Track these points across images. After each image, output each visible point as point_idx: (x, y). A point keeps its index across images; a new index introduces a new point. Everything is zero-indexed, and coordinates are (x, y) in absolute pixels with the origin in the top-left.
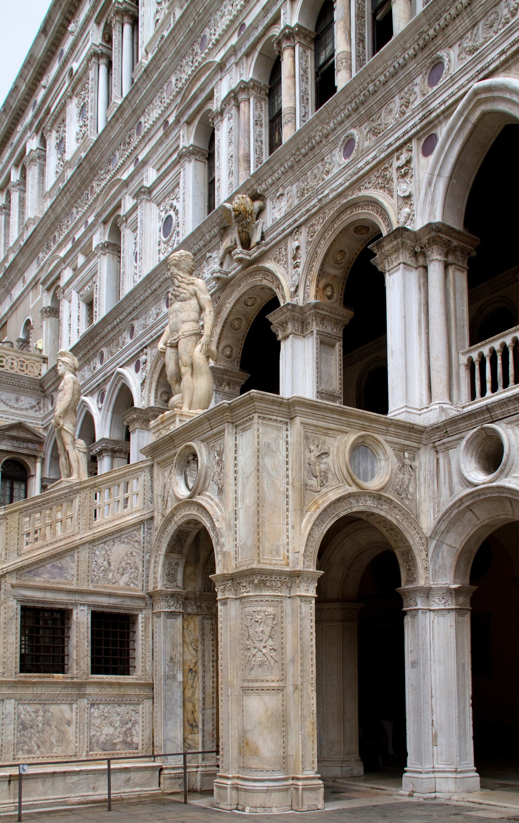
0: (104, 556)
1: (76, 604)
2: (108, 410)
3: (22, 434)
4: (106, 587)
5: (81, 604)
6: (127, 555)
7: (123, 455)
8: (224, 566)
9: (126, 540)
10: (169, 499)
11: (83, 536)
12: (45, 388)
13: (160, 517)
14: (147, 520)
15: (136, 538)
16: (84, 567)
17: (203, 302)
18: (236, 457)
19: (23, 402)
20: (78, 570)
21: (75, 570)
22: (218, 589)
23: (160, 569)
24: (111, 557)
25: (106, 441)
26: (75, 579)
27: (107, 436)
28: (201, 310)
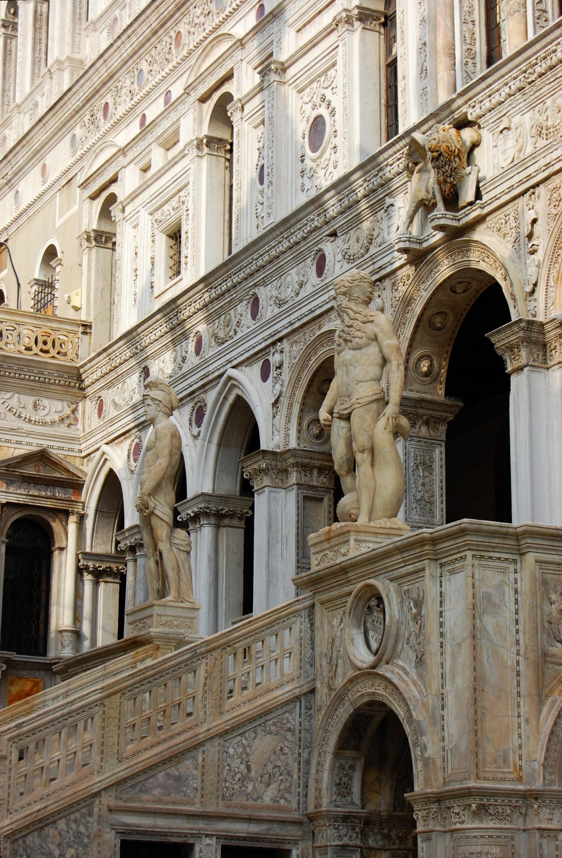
0: (240, 756)
1: (198, 836)
2: (209, 442)
3: (44, 472)
4: (244, 807)
5: (207, 836)
6: (275, 753)
7: (236, 522)
8: (427, 781)
9: (273, 728)
10: (340, 662)
11: (210, 726)
12: (86, 383)
13: (326, 690)
14: (305, 694)
15: (289, 725)
16: (211, 776)
17: (386, 351)
18: (441, 612)
19: (47, 410)
20: (203, 781)
21: (199, 780)
22: (419, 815)
23: (326, 775)
24: (251, 758)
25: (208, 498)
26: (199, 795)
27: (208, 488)
28: (385, 361)
